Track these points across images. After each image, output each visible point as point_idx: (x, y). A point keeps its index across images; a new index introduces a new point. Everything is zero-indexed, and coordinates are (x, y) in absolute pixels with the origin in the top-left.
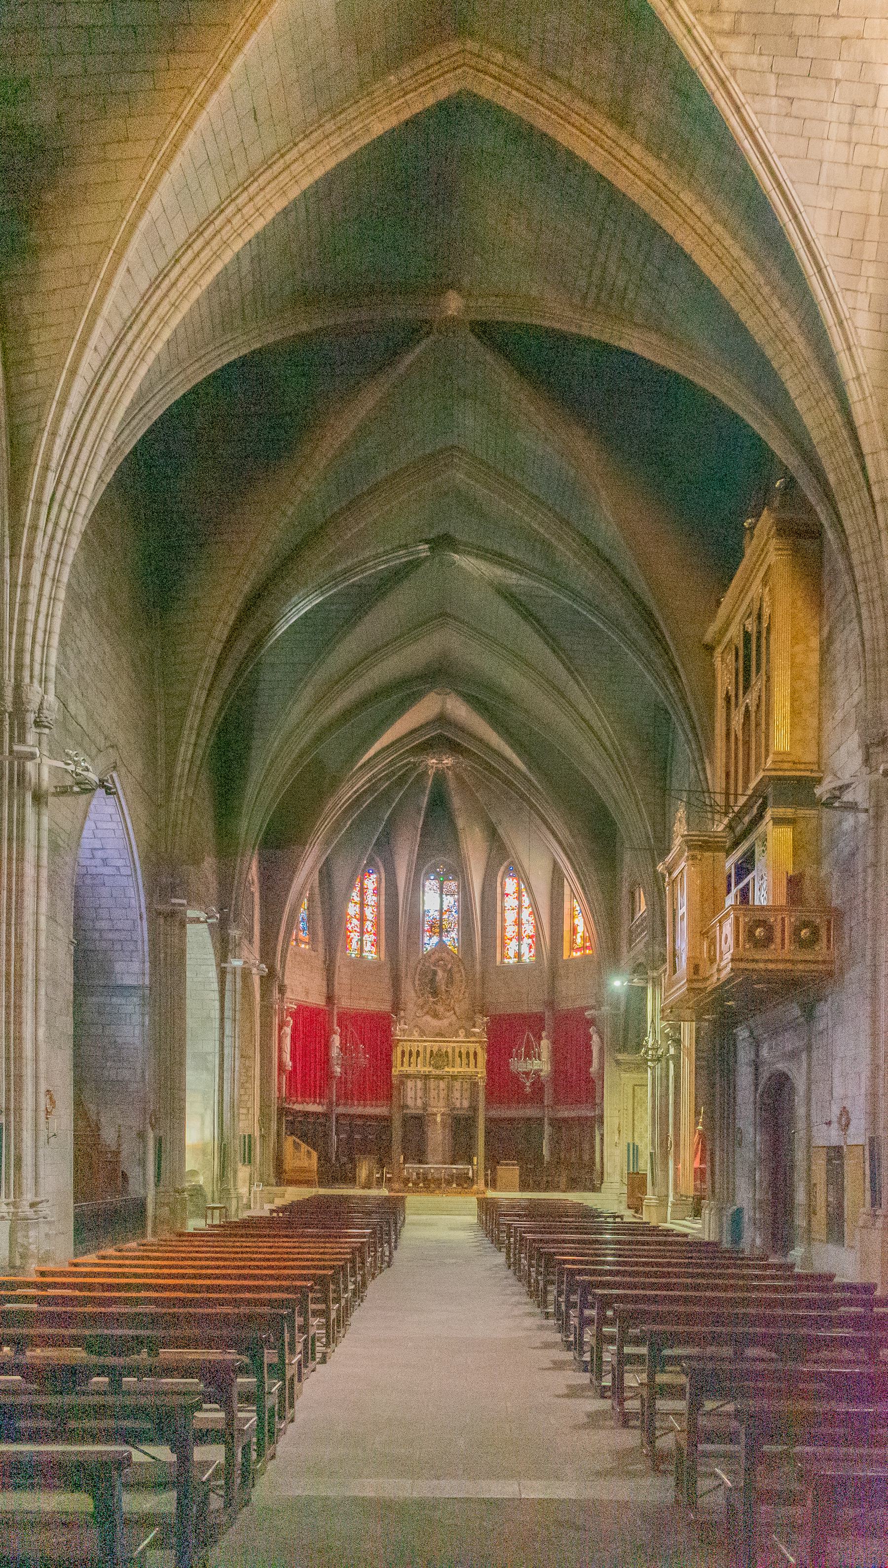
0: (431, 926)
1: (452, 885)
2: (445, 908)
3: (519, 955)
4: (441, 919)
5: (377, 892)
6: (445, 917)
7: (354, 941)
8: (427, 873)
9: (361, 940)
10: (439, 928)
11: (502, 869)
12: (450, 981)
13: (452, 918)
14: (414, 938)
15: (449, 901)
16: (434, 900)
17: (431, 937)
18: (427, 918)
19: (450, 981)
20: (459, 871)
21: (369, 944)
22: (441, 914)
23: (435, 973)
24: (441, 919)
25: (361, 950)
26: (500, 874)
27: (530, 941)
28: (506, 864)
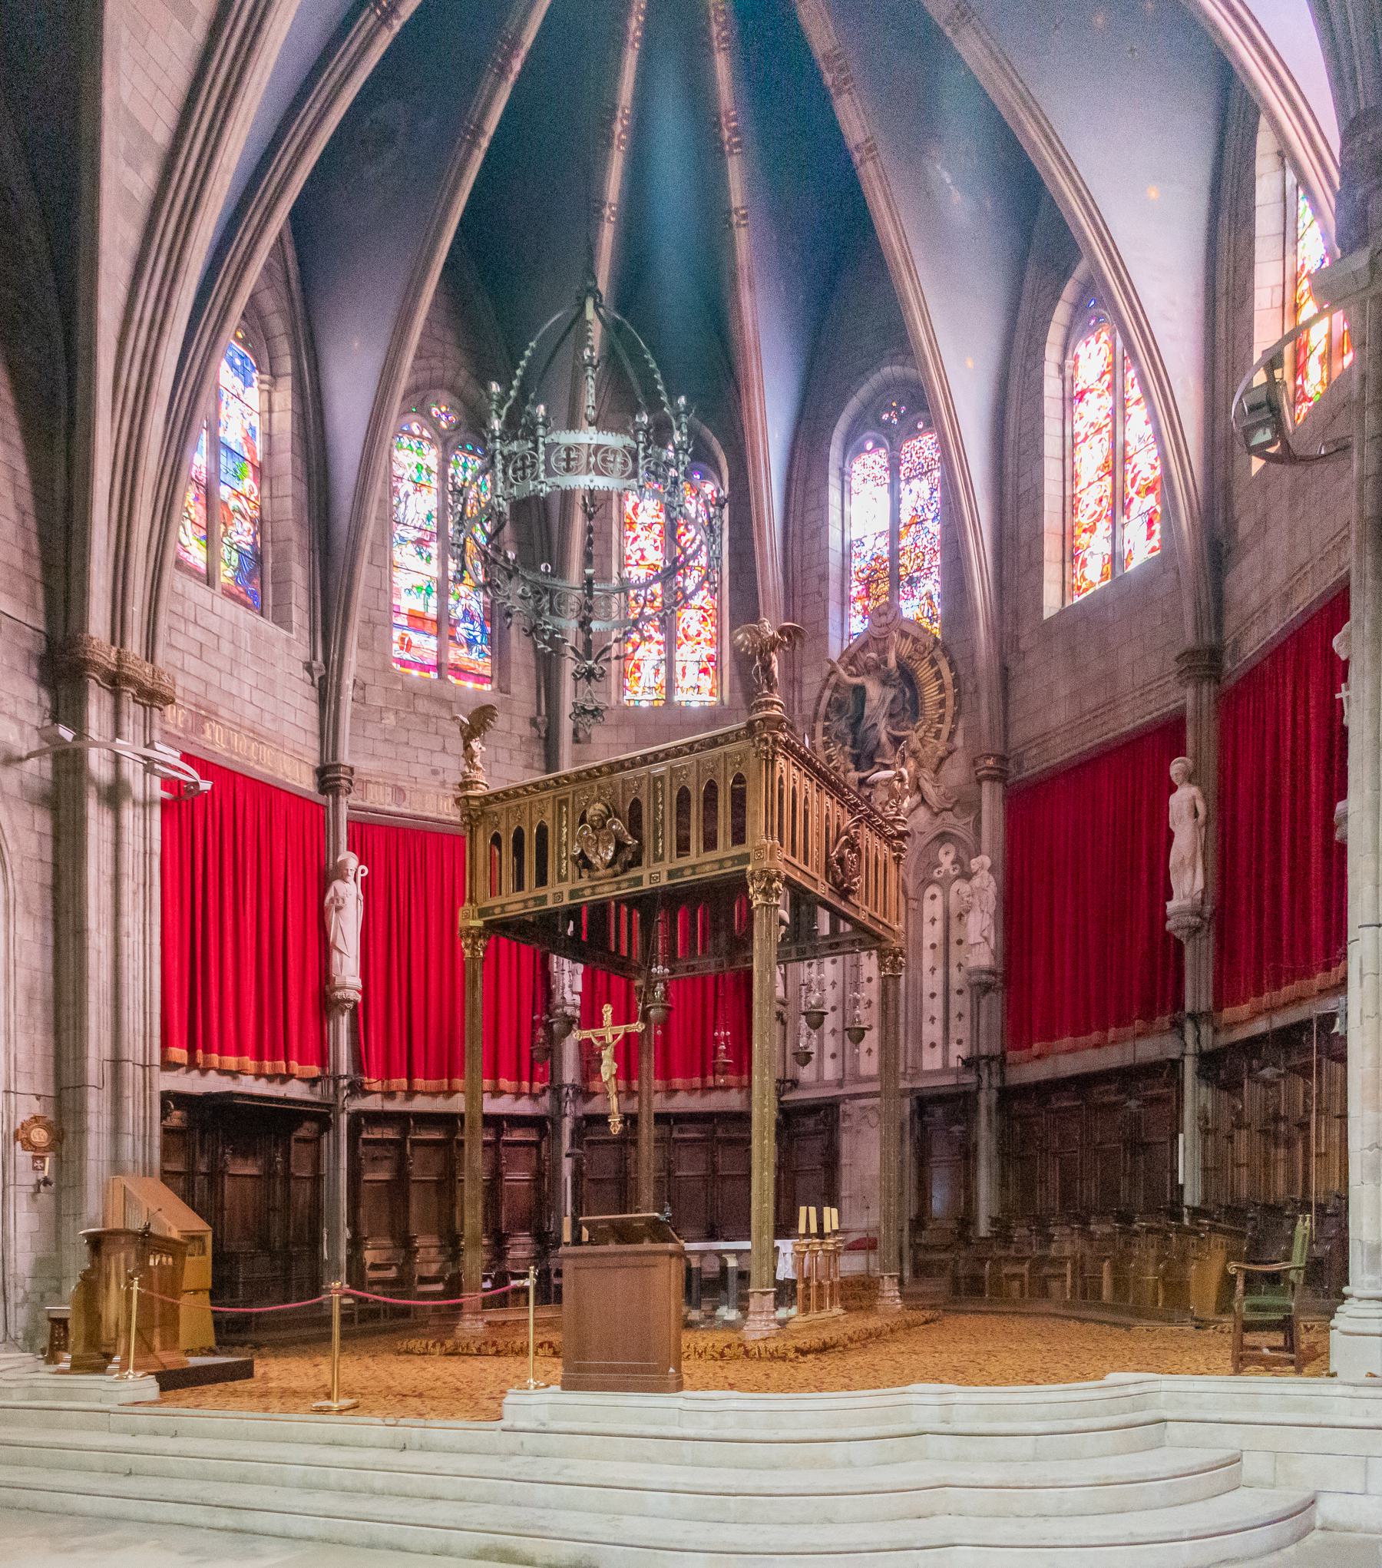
0: (868, 582)
2: (905, 518)
4: (895, 553)
6: (905, 542)
7: (647, 671)
9: (670, 663)
10: (891, 575)
11: (1061, 313)
12: (908, 706)
15: (919, 493)
18: (857, 564)
19: (908, 706)
21: (693, 669)
22: (894, 535)
23: (860, 691)
24: (895, 553)
25: (670, 685)
28: (1069, 291)
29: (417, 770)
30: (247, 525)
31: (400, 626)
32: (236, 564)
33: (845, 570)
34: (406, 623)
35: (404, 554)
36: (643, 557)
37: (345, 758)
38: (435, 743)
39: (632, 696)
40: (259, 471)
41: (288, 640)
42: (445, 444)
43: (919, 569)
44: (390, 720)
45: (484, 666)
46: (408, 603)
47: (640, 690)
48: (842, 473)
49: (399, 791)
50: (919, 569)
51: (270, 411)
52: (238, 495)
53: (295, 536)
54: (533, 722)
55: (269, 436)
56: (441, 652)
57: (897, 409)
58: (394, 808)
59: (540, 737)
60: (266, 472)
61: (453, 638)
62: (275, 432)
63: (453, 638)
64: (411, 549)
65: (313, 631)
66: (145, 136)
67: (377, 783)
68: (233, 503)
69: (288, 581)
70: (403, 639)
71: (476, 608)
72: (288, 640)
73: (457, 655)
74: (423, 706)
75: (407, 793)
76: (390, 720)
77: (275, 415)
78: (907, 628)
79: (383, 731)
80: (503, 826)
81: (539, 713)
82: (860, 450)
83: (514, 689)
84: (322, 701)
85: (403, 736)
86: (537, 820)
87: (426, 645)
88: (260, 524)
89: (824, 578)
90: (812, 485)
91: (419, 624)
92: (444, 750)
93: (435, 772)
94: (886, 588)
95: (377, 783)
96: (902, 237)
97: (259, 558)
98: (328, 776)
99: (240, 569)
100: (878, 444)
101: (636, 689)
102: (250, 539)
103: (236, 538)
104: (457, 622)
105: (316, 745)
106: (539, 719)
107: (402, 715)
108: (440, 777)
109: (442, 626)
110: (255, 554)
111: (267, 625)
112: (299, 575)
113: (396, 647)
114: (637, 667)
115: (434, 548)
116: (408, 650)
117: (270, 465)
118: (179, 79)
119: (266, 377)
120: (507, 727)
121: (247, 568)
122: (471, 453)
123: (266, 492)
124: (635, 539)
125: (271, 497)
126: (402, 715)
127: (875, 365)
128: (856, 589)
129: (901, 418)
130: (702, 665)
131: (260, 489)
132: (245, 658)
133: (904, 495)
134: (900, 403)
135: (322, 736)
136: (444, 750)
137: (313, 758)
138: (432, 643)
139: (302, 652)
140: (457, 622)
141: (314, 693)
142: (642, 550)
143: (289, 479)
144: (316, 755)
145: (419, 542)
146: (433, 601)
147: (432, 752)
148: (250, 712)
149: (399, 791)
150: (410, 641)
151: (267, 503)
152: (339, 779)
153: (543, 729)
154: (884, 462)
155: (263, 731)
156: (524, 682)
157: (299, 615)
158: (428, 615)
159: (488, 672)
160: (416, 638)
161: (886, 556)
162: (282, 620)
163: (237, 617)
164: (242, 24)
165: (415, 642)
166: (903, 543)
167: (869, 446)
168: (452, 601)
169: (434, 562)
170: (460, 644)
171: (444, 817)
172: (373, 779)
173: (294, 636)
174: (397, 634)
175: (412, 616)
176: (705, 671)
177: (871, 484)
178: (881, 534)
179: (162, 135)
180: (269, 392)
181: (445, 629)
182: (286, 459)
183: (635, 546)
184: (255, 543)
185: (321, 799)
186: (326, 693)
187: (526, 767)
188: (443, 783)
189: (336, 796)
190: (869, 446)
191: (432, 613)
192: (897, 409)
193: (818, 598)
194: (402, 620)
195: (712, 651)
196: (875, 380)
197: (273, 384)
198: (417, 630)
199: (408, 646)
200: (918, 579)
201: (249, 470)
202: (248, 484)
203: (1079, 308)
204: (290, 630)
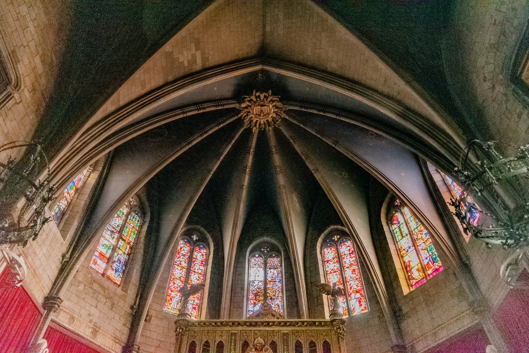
0: (256, 295)
1: (275, 261)
3: (349, 311)
4: (265, 289)
5: (205, 263)
8: (251, 252)
10: (264, 294)
11: (320, 240)
13: (277, 287)
14: (237, 304)
16: (259, 273)
17: (255, 304)
18: (252, 288)
20: (282, 247)
22: (265, 283)
24: (265, 289)
26: (319, 245)
27: (358, 295)
29: (83, 312)
30: (66, 202)
31: (96, 256)
32: (56, 211)
33: (248, 290)
34: (98, 255)
35: (107, 234)
36: (180, 264)
37: (61, 295)
38: (94, 303)
39: (167, 310)
40: (77, 190)
41: (62, 243)
42: (131, 208)
43: (274, 296)
44: (81, 287)
45: (118, 280)
46: (101, 249)
47: (170, 308)
48: (249, 261)
49: (72, 318)
50: (274, 296)
51: (88, 177)
52: (68, 193)
53: (80, 211)
54: (132, 308)
55: (85, 183)
56: (106, 270)
57: (267, 249)
58: (67, 326)
59: (132, 314)
60: (79, 191)
61: (111, 266)
62: (87, 182)
63: (111, 266)
64: (109, 233)
65: (71, 245)
66: (119, 101)
67: (66, 312)
68: (66, 194)
69: (71, 224)
70: (94, 260)
71: (123, 260)
72: (62, 243)
73: (111, 273)
74: (95, 286)
75: (75, 320)
76: (81, 287)
77: (89, 179)
78: (274, 313)
79: (77, 291)
80: (197, 338)
81: (135, 304)
82: (254, 256)
83: (129, 292)
84: (62, 270)
85: (84, 296)
86: (218, 339)
87: (101, 265)
88: (69, 204)
89: (243, 289)
90: (241, 260)
91: (102, 257)
92: (96, 307)
93: (89, 315)
94: (262, 299)
95: (66, 312)
96: (289, 207)
97: (63, 214)
98: (51, 301)
99: (56, 214)
100: (260, 256)
101: (169, 307)
102: (64, 207)
103: (60, 204)
104: (115, 262)
105: (50, 287)
106: (135, 307)
107: (87, 287)
108: (90, 318)
109: (109, 260)
110: (63, 211)
111: (59, 235)
112: (75, 224)
113: (92, 262)
114: (171, 299)
115: (116, 236)
116: (95, 265)
117: (82, 190)
118: (133, 96)
119: (92, 169)
120: (122, 306)
121: (58, 215)
122: (137, 214)
123: (76, 196)
124: (179, 258)
125: (77, 198)
126: (87, 287)
127: (262, 235)
128: (251, 296)
129: (268, 251)
130: (194, 306)
131: (75, 195)
132: (47, 243)
133: (269, 272)
134: (268, 248)
135: (54, 284)
136: (96, 307)
137: (46, 291)
138: (104, 265)
139: (64, 249)
140: (115, 262)
141: (60, 266)
142: (181, 262)
143: (87, 196)
144: (48, 291)
145: (112, 232)
146: (110, 252)
147: (92, 306)
148: (38, 263)
149: (72, 318)
150: (96, 262)
151: (75, 199)
152: (55, 304)
153: (135, 311)
154: (262, 261)
155: (37, 272)
156: (133, 291)
157: (69, 237)
158: (106, 256)
159: (119, 283)
160: (99, 262)
161: (262, 288)
162: (64, 237)
163: (53, 227)
164: (149, 99)
165: (98, 263)
166: (268, 286)
167: (257, 256)
168: (116, 254)
169: (115, 240)
170: (113, 269)
171: (85, 336)
172: (64, 310)
173: (64, 243)
174: (94, 257)
175: (101, 254)
176: (194, 308)
177: (257, 266)
178: (261, 281)
179: (122, 103)
180: (91, 173)
181: (111, 262)
182: (88, 191)
183: (178, 260)
184: (65, 209)
185: (41, 310)
186: (65, 269)
187: (123, 325)
188: (91, 321)
189: (49, 311)
190: (257, 256)
191: (108, 255)
192: (267, 249)
193: (240, 295)
194: (97, 254)
195: (198, 302)
196: (262, 239)
197: (93, 171)
198: (101, 259)
199: (95, 263)
200: (274, 299)
201: (74, 188)
202: (72, 192)
203: (324, 241)
204: (64, 240)
